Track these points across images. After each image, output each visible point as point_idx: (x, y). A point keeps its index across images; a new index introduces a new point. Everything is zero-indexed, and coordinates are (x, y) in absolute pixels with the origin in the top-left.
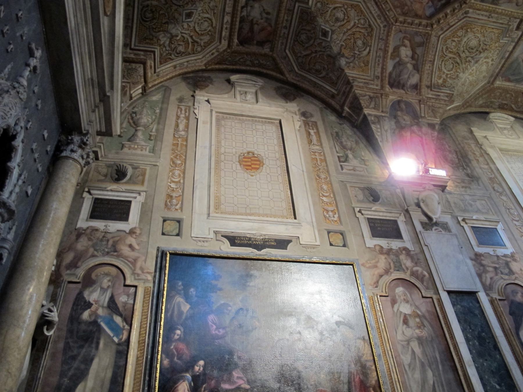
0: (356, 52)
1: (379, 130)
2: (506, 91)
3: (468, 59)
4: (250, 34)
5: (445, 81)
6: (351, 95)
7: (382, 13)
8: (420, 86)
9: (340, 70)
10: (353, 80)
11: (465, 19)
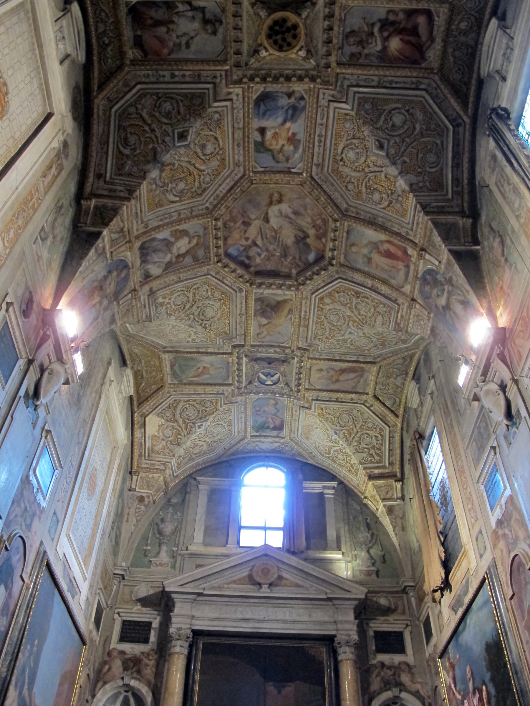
0: (170, 185)
1: (91, 262)
2: (160, 368)
4: (149, 22)
5: (162, 304)
6: (117, 202)
7: (222, 199)
8: (150, 281)
9: (142, 174)
10: (137, 197)
11: (233, 292)
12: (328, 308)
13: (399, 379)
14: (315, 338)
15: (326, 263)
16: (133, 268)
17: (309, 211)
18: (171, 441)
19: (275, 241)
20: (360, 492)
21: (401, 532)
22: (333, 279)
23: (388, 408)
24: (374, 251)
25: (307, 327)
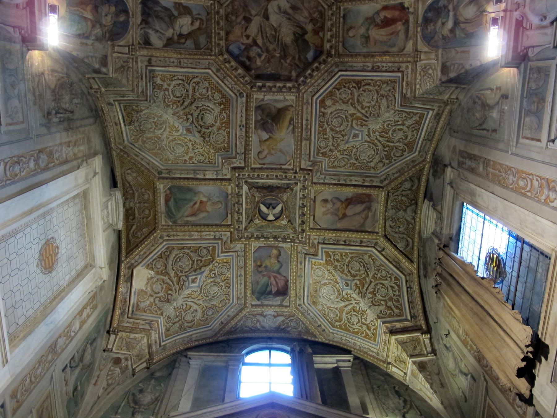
2: (154, 204)
3: (189, 116)
5: (160, 87)
8: (151, 48)
11: (233, 95)
12: (329, 111)
13: (409, 210)
14: (318, 155)
15: (324, 57)
16: (133, 17)
17: (306, 5)
18: (160, 298)
19: (275, 41)
20: (381, 361)
21: (441, 389)
22: (333, 74)
23: (401, 251)
24: (371, 27)
25: (309, 139)
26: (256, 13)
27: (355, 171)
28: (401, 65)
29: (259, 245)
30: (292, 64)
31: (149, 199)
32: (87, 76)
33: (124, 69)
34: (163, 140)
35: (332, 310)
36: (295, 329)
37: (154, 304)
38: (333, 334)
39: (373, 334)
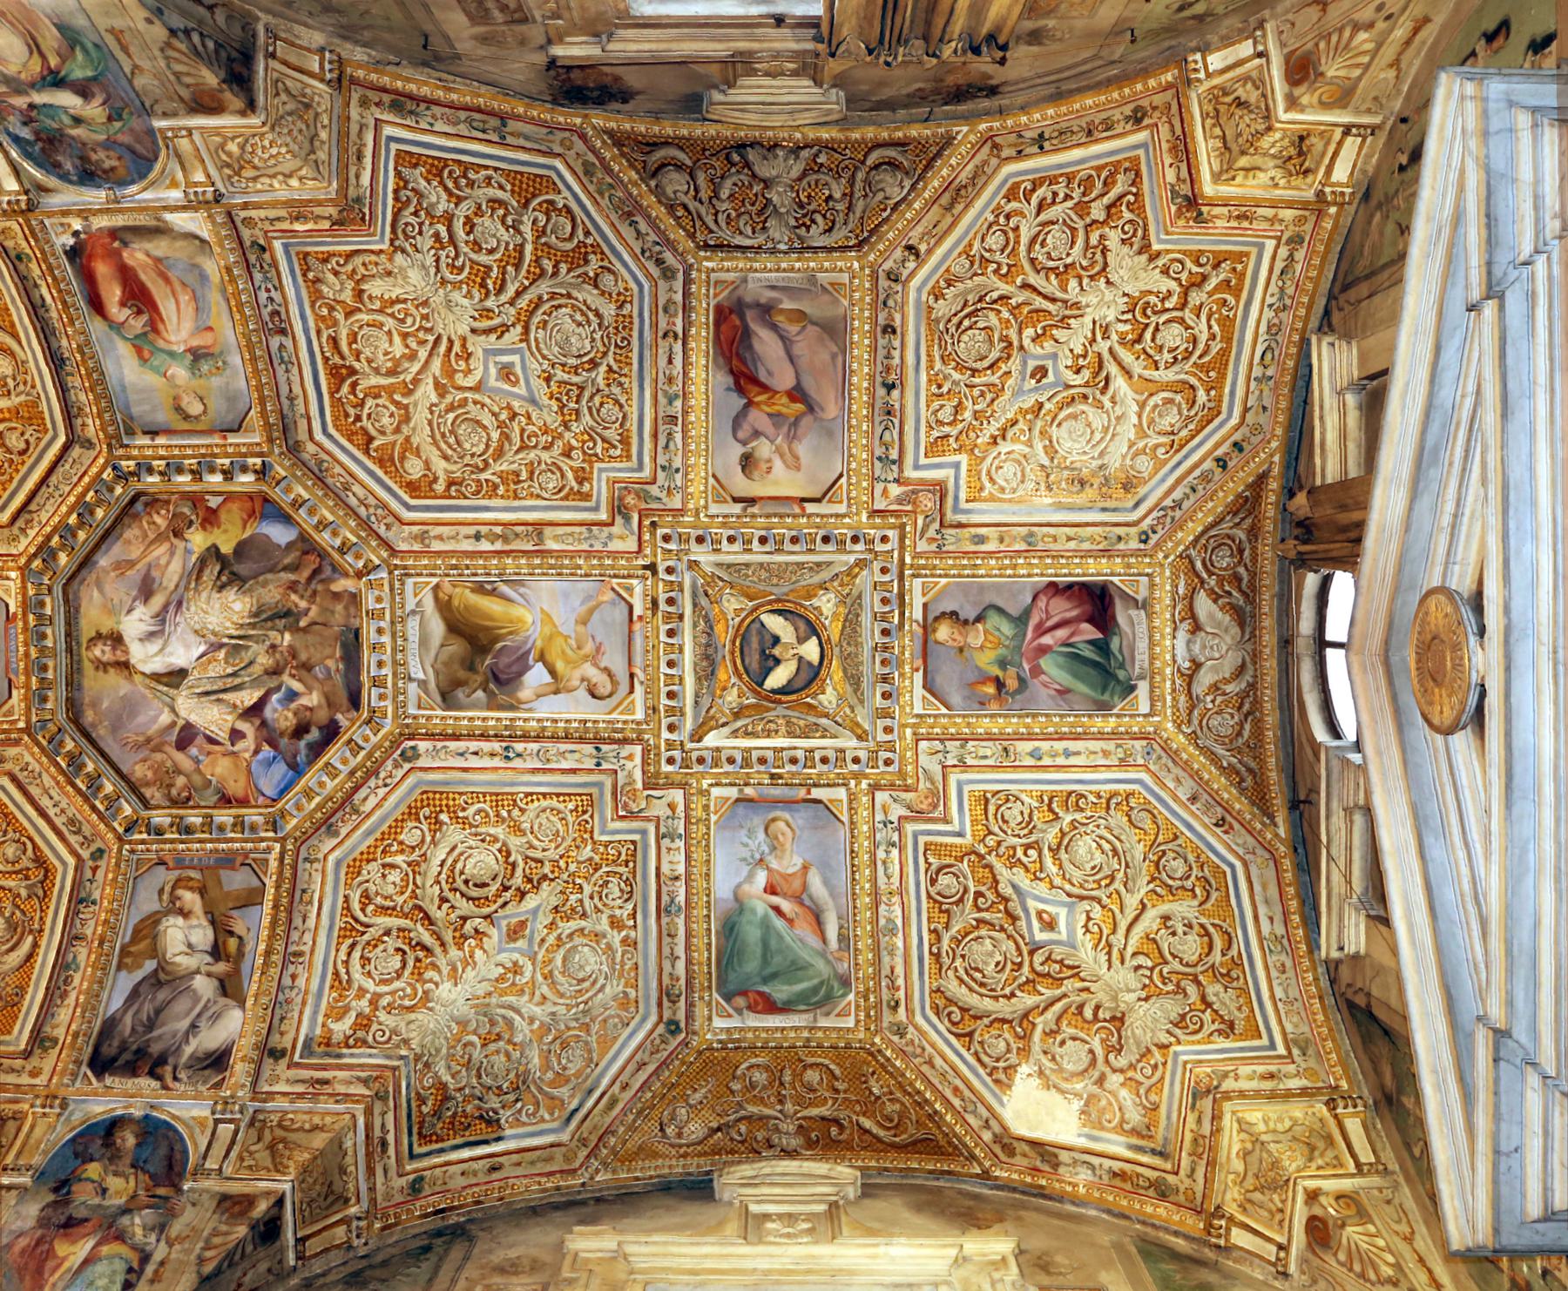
3: (469, 927)
5: (364, 1022)
12: (440, 466)
14: (586, 497)
17: (134, 555)
22: (325, 457)
26: (166, 710)
27: (635, 366)
28: (248, 243)
29: (919, 691)
30: (309, 592)
31: (767, 1068)
32: (292, 1263)
33: (283, 1140)
34: (553, 1014)
35: (1151, 422)
36: (1241, 551)
37: (1130, 1074)
38: (1246, 410)
39: (1216, 266)
